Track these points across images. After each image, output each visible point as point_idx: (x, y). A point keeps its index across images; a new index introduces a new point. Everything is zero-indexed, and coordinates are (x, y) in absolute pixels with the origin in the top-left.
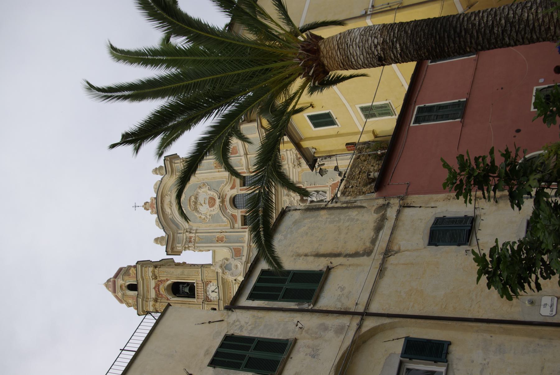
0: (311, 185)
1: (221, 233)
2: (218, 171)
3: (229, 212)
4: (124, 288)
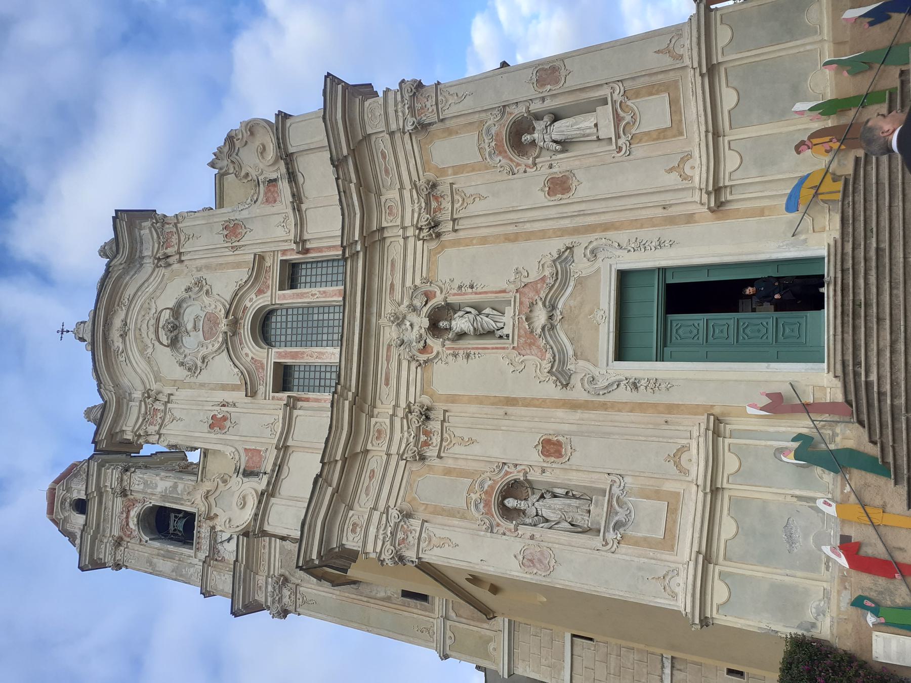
1: (224, 405)
3: (247, 355)
4: (67, 504)
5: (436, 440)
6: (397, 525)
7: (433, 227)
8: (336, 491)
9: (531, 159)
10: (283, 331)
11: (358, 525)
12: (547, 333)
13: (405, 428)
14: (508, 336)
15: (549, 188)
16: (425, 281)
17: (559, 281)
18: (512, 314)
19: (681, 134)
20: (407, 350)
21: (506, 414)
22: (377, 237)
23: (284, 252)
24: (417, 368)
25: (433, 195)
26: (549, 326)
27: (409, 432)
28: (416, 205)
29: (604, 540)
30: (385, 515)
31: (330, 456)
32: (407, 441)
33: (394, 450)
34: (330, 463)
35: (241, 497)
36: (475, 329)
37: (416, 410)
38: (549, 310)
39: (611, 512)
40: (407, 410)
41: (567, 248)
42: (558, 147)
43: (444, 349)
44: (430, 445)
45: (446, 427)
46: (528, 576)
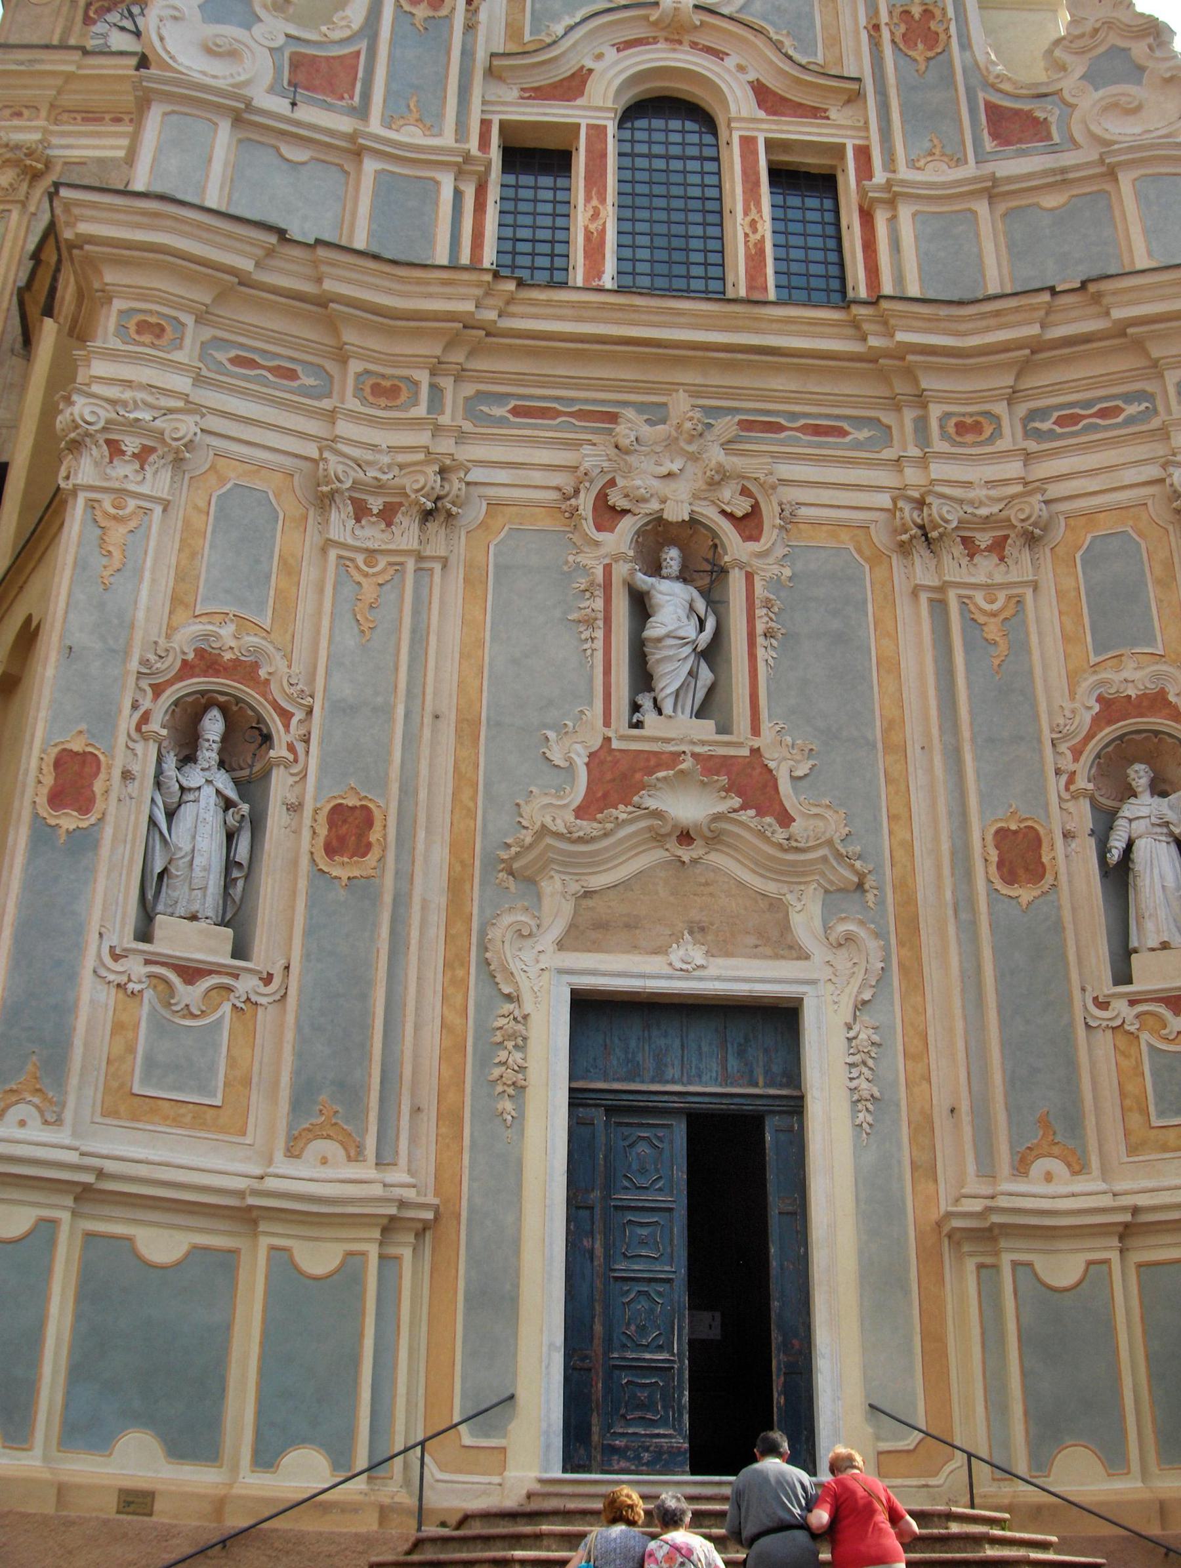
0: (768, 604)
2: (877, 27)
3: (599, 57)
5: (372, 535)
6: (160, 435)
7: (925, 535)
8: (244, 280)
9: (1090, 786)
10: (657, 149)
11: (158, 337)
12: (642, 824)
13: (401, 458)
14: (639, 725)
15: (1015, 832)
16: (786, 513)
17: (780, 855)
18: (696, 737)
19: (1132, 1149)
20: (605, 464)
21: (437, 717)
22: (901, 387)
23: (863, 153)
24: (558, 489)
25: (1006, 537)
26: (663, 831)
27: (390, 466)
28: (981, 493)
29: (125, 950)
30: (180, 404)
31: (332, 264)
32: (369, 463)
33: (344, 428)
34: (315, 264)
35: (236, 45)
36: (659, 640)
37: (447, 486)
38: (705, 830)
39: (191, 973)
40: (448, 462)
41: (862, 876)
42: (1115, 856)
43: (607, 561)
44: (358, 520)
45: (401, 564)
46: (34, 763)
